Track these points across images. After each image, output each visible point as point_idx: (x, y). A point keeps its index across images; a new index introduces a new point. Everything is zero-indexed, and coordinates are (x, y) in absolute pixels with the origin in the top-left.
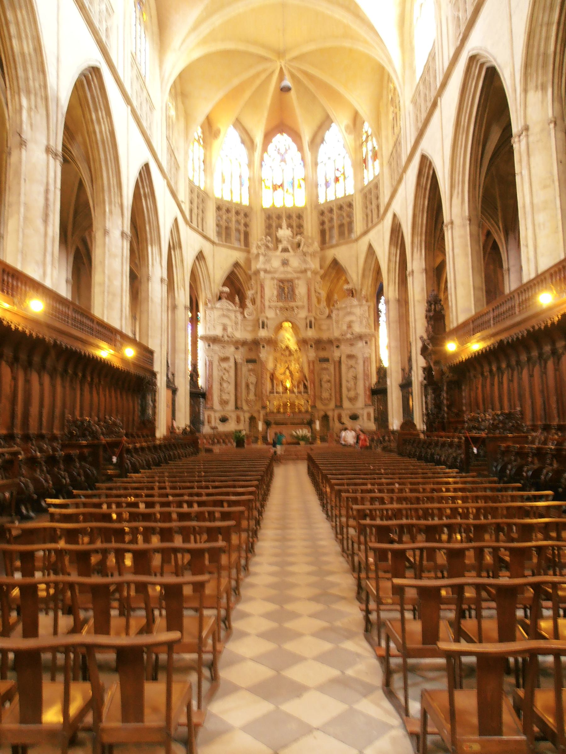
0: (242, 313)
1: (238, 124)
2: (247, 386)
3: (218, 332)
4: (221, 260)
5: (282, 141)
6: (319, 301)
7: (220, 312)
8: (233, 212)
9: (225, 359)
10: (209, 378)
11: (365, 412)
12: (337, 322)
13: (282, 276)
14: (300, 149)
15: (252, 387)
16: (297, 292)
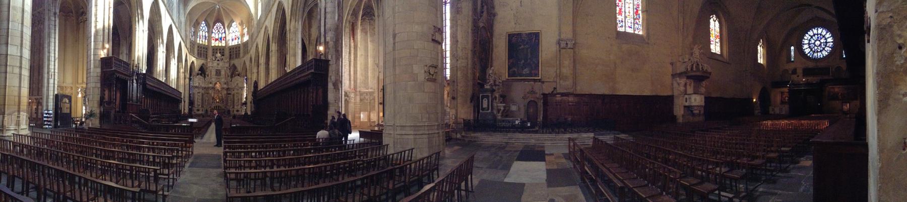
1: (206, 21)
5: (218, 24)
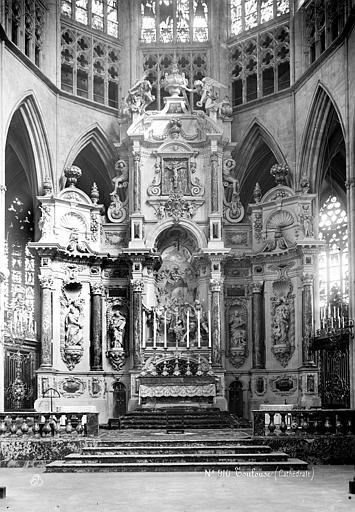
2: (111, 333)
6: (229, 197)
9: (74, 287)
11: (304, 377)
12: (259, 227)
15: (119, 336)
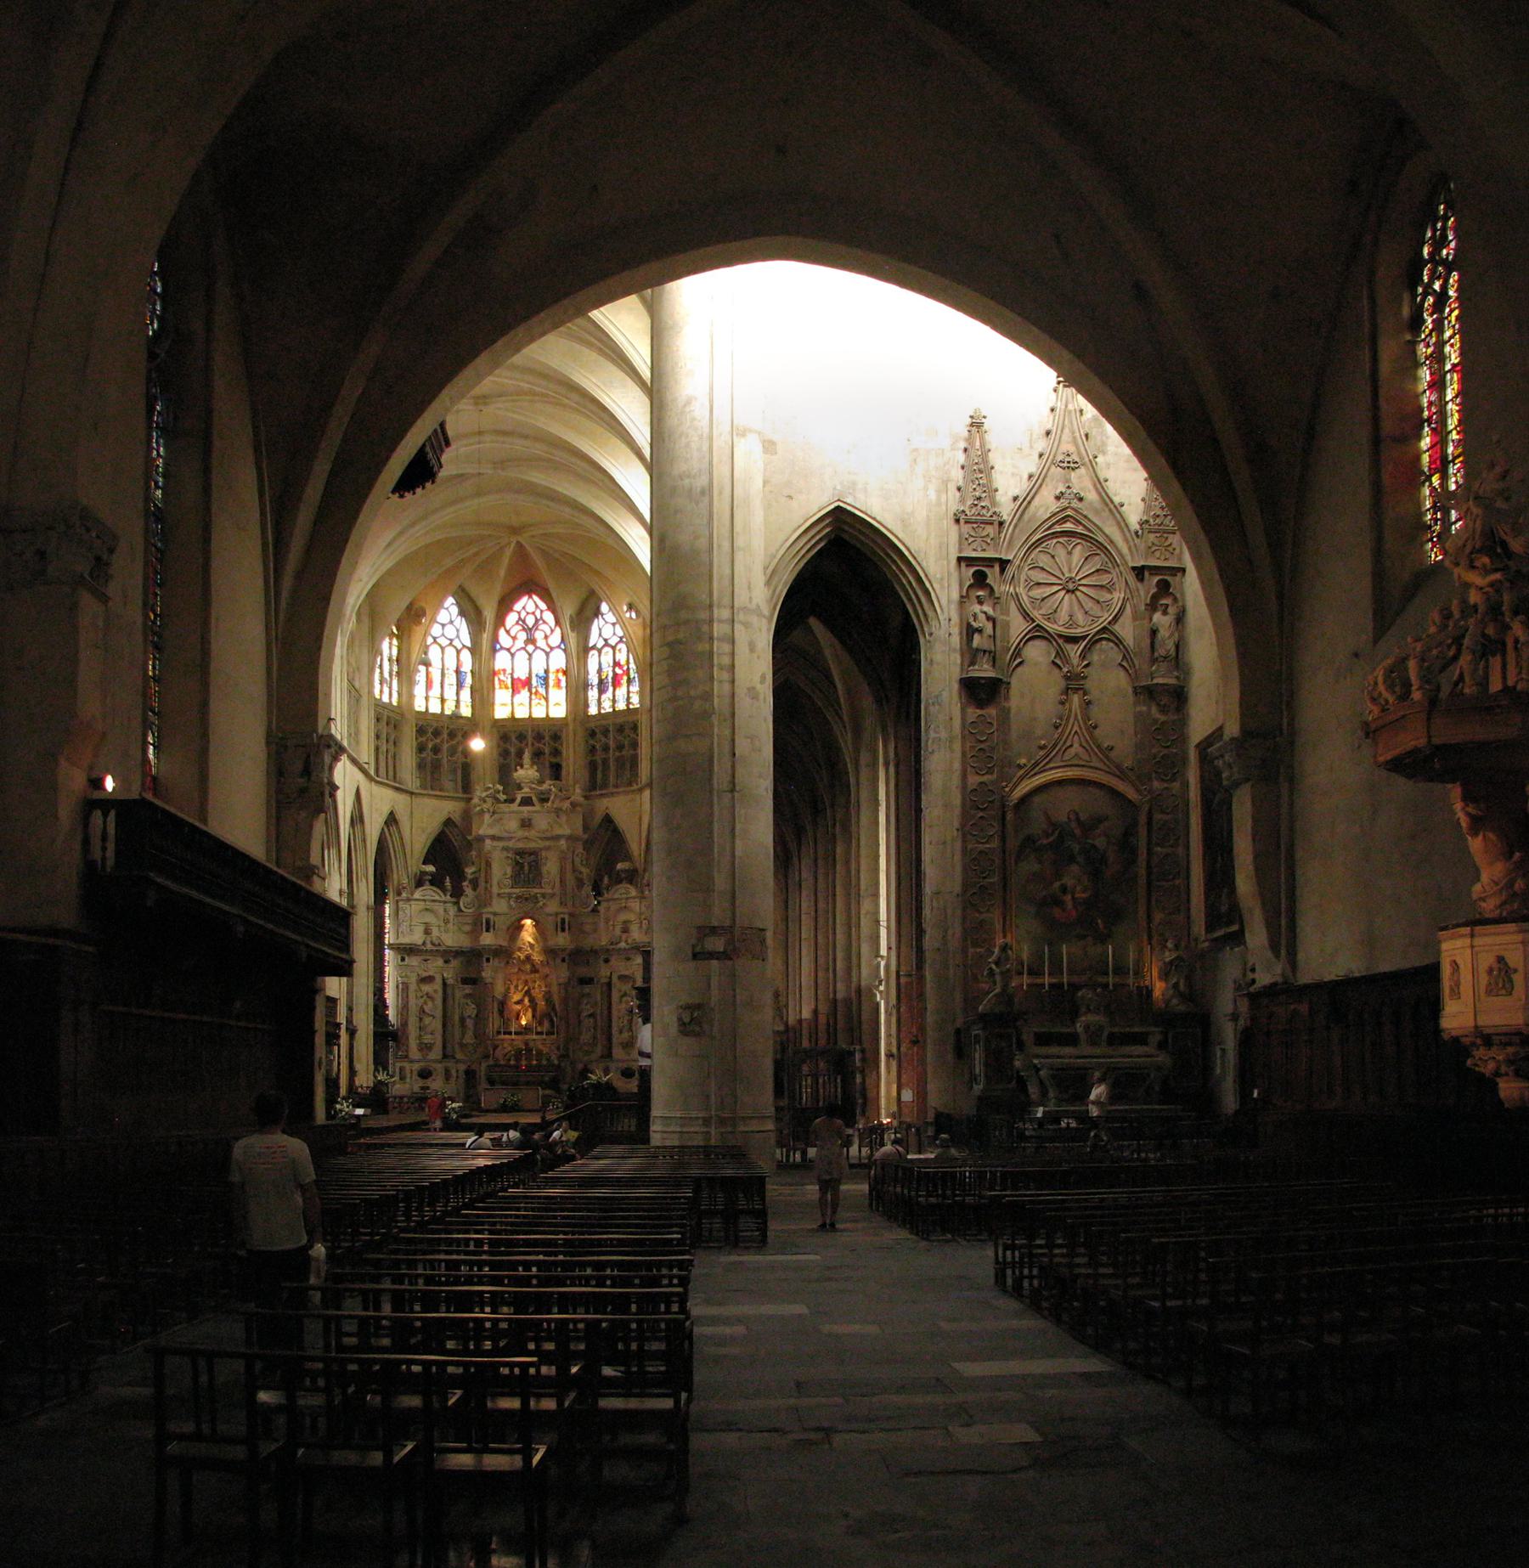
0: (457, 903)
3: (417, 937)
4: (424, 817)
5: (529, 605)
6: (580, 883)
7: (422, 905)
8: (445, 732)
10: (404, 1009)
13: (520, 845)
14: (558, 623)
15: (470, 1023)
16: (544, 870)
